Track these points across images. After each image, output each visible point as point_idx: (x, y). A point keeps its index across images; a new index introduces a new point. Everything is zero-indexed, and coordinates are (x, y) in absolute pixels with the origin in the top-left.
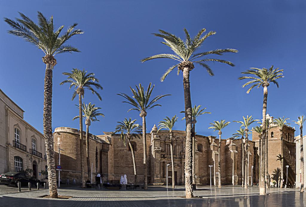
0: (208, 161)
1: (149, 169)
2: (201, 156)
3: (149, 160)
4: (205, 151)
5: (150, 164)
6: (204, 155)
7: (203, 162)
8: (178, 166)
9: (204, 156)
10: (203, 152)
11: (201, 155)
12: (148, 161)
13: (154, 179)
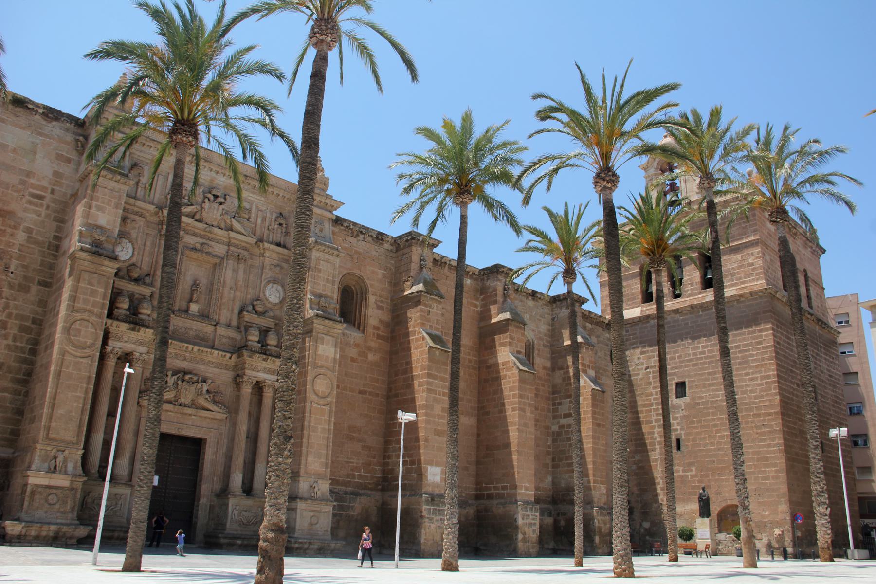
0: (390, 390)
1: (16, 392)
2: (353, 352)
3: (34, 321)
4: (377, 328)
5: (34, 352)
6: (370, 349)
7: (361, 392)
8: (215, 402)
9: (371, 357)
10: (370, 330)
11: (357, 345)
12: (28, 324)
13: (26, 485)
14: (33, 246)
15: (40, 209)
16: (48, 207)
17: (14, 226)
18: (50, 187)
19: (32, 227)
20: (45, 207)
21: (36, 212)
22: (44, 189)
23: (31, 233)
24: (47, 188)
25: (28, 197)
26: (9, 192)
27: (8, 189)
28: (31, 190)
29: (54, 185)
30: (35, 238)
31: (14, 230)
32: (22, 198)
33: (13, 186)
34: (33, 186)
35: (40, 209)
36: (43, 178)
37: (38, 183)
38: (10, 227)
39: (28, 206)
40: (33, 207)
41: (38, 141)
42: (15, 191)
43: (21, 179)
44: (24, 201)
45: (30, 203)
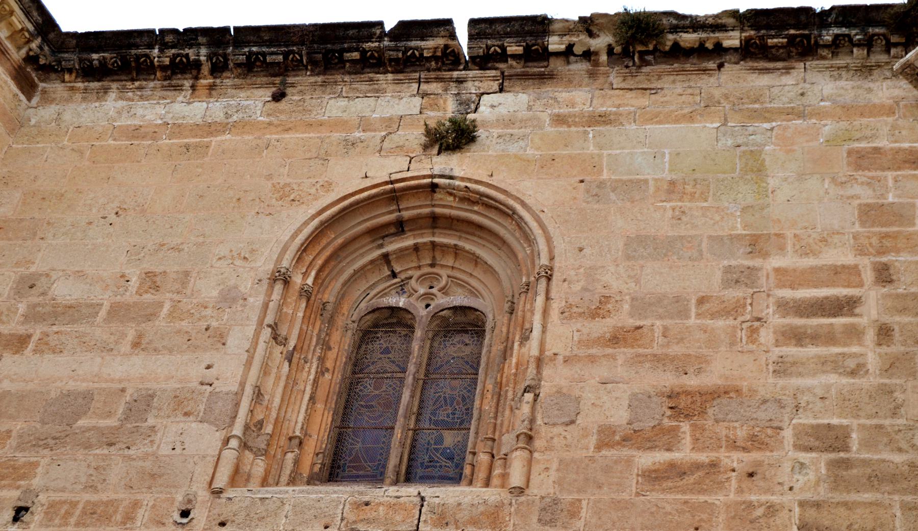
14: (867, 496)
15: (855, 349)
16: (884, 333)
17: (753, 438)
18: (866, 264)
19: (835, 421)
20: (870, 336)
21: (833, 365)
22: (838, 273)
23: (846, 449)
24: (854, 270)
25: (776, 320)
26: (692, 321)
27: (684, 314)
28: (787, 293)
29: (881, 252)
30: (865, 463)
31: (755, 455)
32: (753, 331)
33: (701, 301)
34: (784, 277)
35: (855, 349)
36: (824, 240)
37: (810, 262)
38: (733, 445)
39: (792, 351)
40: (812, 351)
41: (758, 138)
42: (713, 316)
43: (728, 270)
44: (766, 336)
45: (798, 337)
